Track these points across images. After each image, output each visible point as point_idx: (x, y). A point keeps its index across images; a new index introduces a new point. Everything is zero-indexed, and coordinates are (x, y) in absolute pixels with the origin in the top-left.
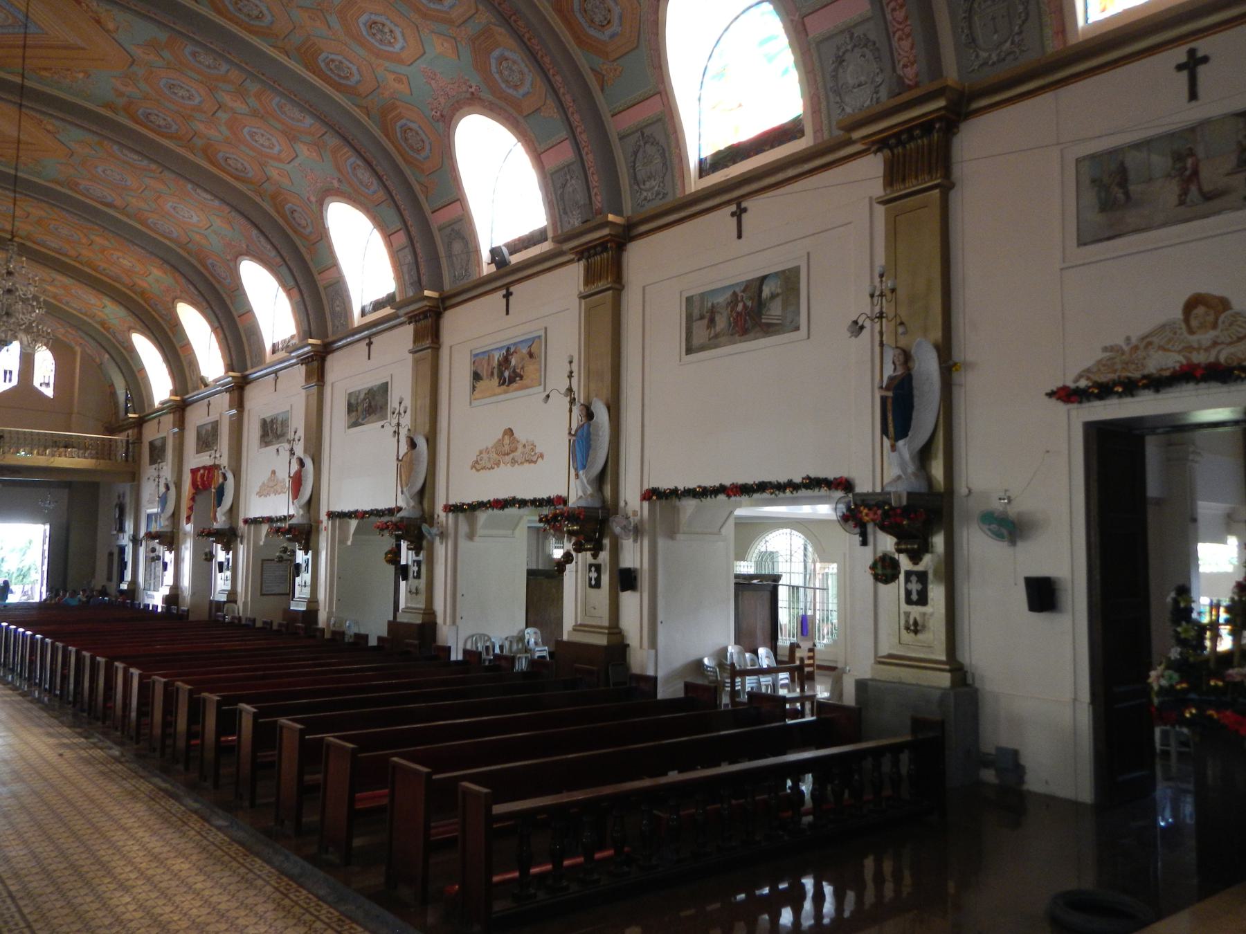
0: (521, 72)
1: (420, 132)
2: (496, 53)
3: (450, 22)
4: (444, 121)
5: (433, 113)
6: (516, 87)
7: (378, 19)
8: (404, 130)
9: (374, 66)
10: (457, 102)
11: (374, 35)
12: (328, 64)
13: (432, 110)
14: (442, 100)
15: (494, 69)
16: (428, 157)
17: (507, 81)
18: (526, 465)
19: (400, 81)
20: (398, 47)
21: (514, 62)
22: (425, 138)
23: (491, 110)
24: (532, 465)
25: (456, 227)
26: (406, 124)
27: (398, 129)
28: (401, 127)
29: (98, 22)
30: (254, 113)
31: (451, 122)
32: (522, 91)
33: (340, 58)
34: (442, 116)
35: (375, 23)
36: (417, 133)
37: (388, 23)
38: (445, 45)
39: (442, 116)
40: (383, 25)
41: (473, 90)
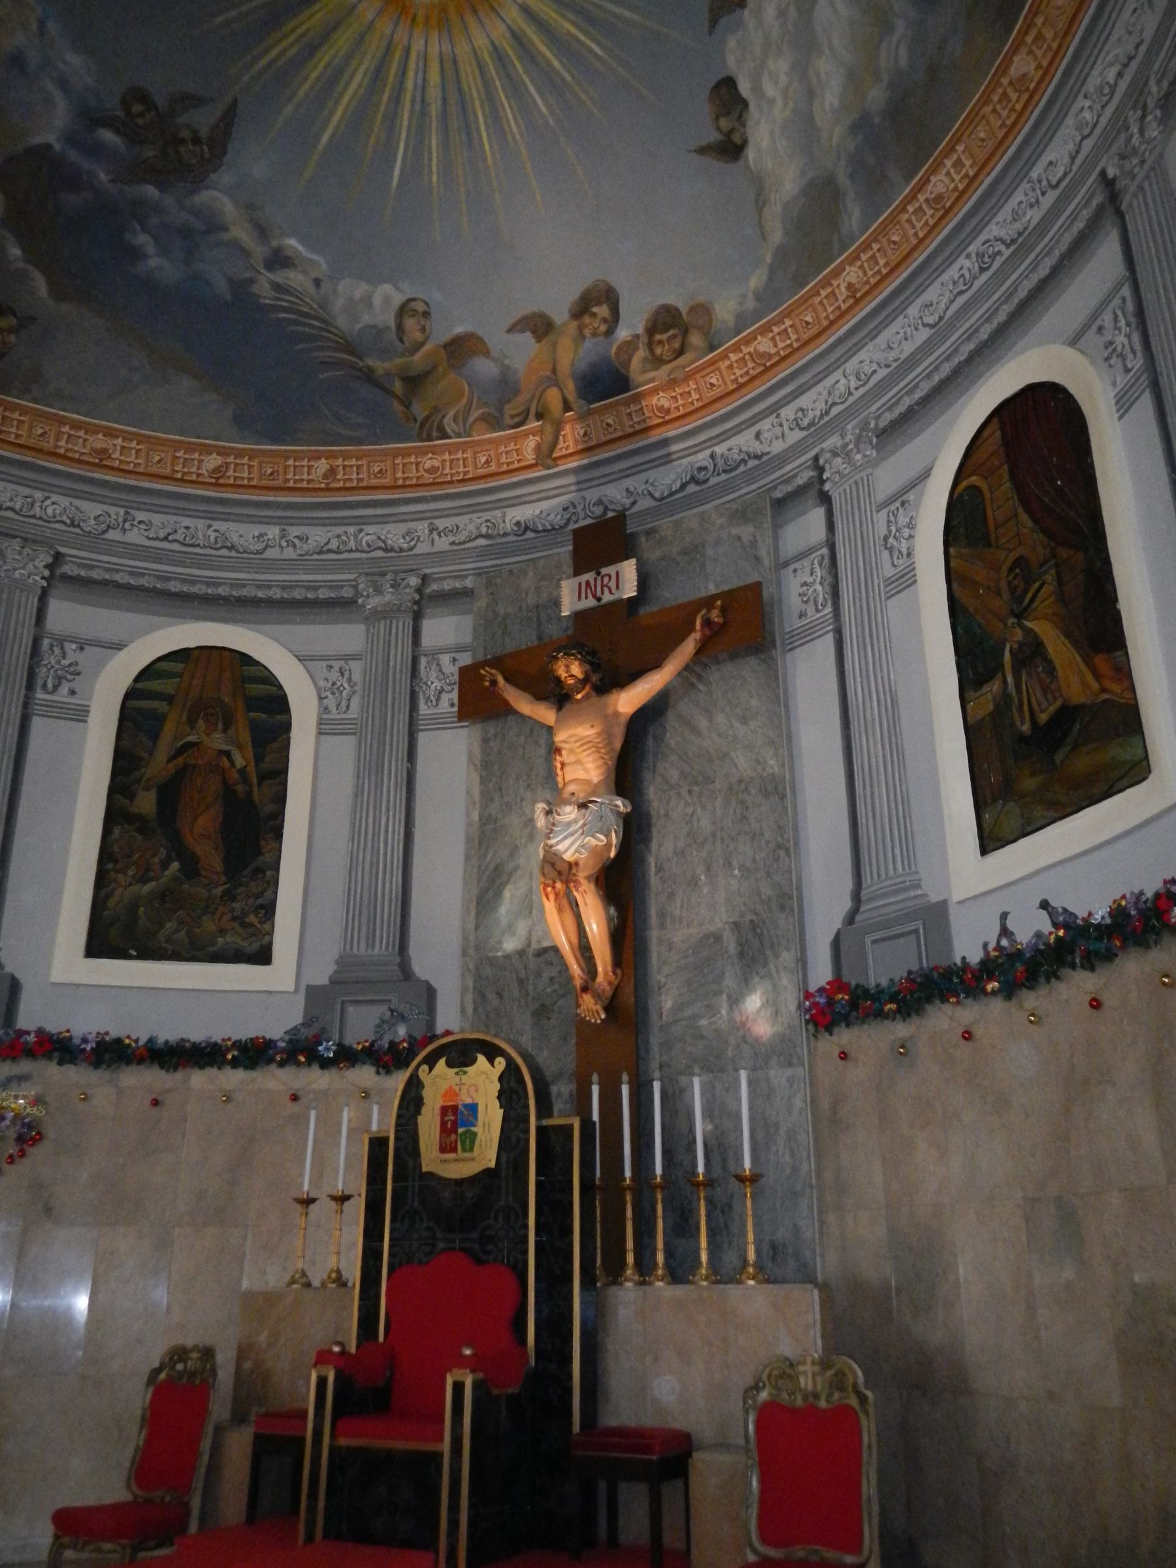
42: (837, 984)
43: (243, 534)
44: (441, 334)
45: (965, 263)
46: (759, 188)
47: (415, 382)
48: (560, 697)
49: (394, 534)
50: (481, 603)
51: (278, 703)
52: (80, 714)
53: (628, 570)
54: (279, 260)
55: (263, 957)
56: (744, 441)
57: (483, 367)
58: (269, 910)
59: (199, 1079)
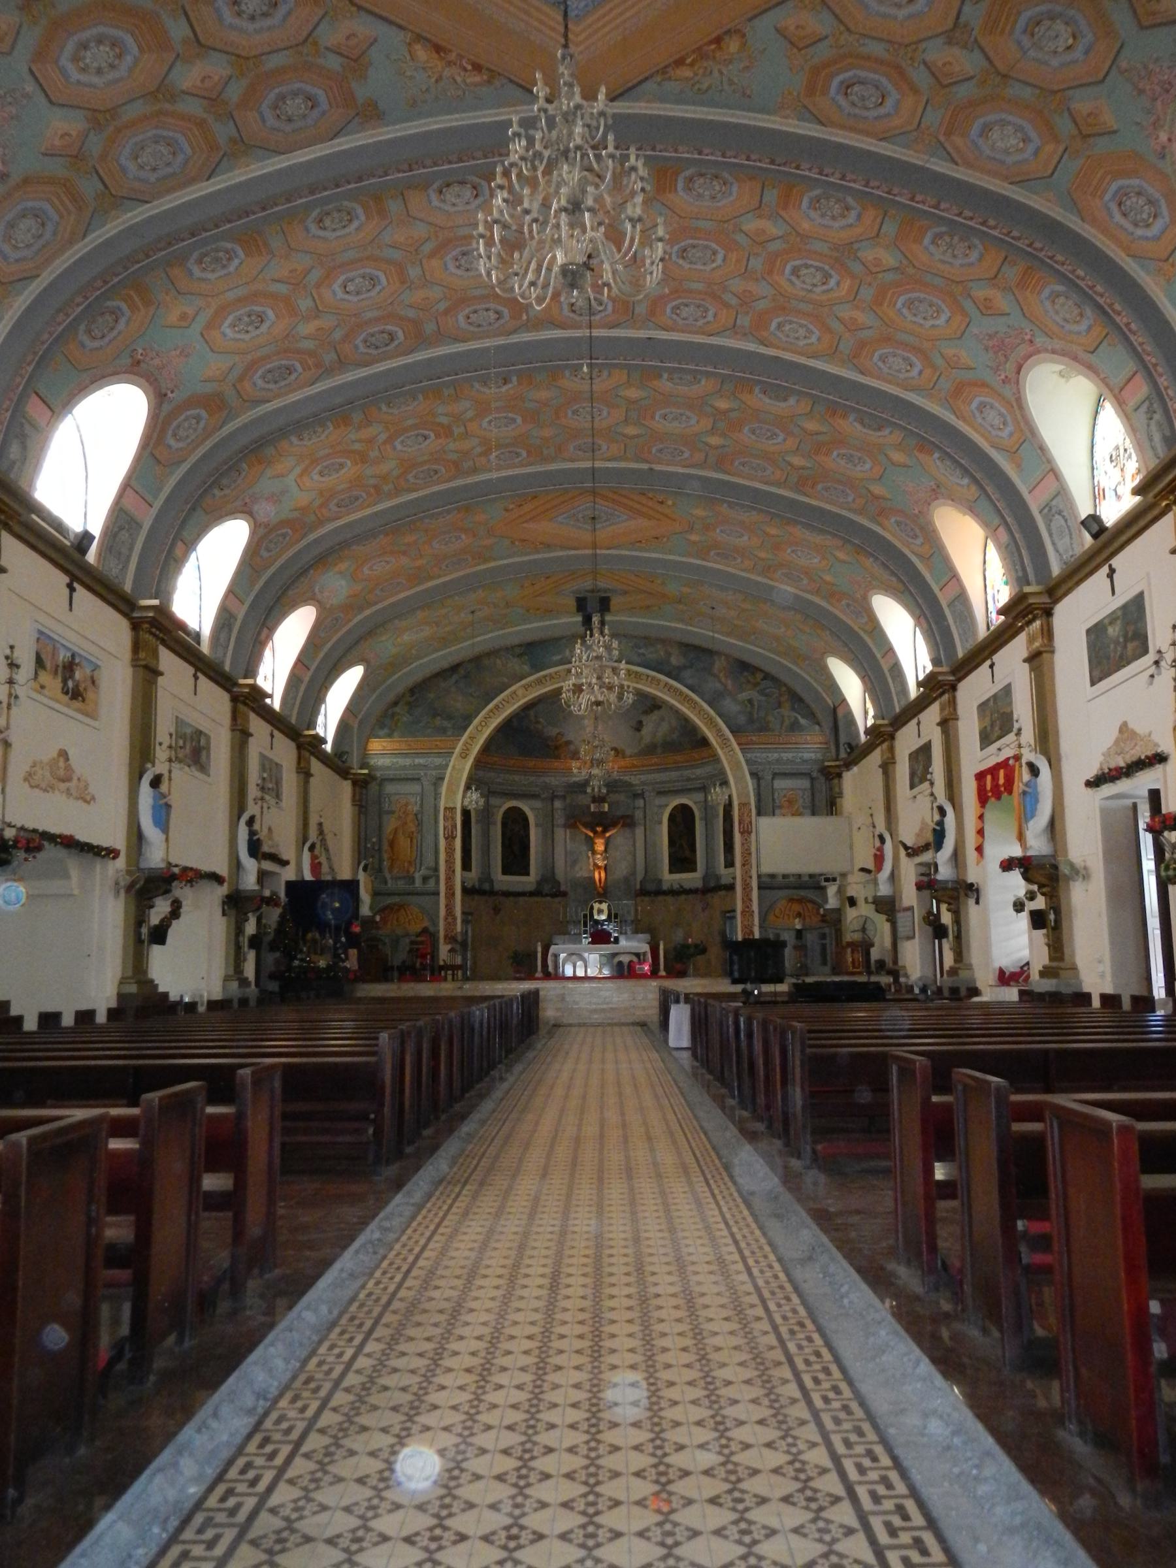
0: (188, 436)
1: (115, 332)
2: (204, 414)
3: (241, 379)
4: (132, 365)
5: (140, 351)
6: (175, 435)
7: (264, 328)
8: (116, 314)
9: (210, 299)
10: (156, 380)
11: (249, 316)
12: (227, 252)
13: (144, 349)
14: (157, 362)
15: (189, 413)
16: (83, 346)
17: (178, 426)
18: (80, 803)
19: (183, 317)
20: (228, 331)
21: (195, 430)
22: (106, 340)
23: (153, 418)
24: (85, 805)
25: (27, 427)
26: (123, 314)
27: (115, 303)
28: (119, 309)
29: (438, 49)
30: (163, 92)
31: (135, 374)
32: (172, 442)
33: (232, 269)
34: (139, 362)
35: (262, 321)
36: (112, 329)
37: (258, 332)
38: (218, 372)
39: (139, 362)
40: (257, 328)
41: (170, 395)
42: (641, 889)
43: (517, 778)
44: (564, 739)
45: (677, 773)
46: (641, 738)
47: (557, 748)
48: (595, 832)
49: (547, 780)
50: (568, 801)
51: (525, 820)
52: (495, 824)
53: (606, 805)
54: (538, 722)
55: (528, 874)
56: (627, 778)
57: (572, 747)
58: (528, 865)
59: (521, 899)
